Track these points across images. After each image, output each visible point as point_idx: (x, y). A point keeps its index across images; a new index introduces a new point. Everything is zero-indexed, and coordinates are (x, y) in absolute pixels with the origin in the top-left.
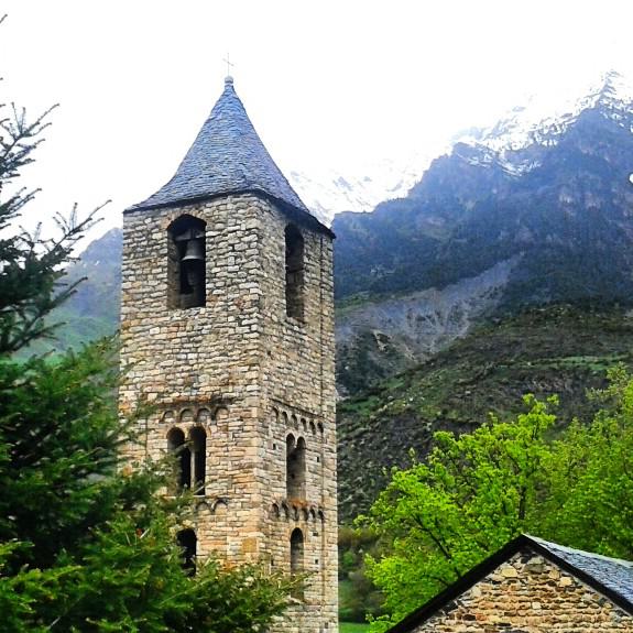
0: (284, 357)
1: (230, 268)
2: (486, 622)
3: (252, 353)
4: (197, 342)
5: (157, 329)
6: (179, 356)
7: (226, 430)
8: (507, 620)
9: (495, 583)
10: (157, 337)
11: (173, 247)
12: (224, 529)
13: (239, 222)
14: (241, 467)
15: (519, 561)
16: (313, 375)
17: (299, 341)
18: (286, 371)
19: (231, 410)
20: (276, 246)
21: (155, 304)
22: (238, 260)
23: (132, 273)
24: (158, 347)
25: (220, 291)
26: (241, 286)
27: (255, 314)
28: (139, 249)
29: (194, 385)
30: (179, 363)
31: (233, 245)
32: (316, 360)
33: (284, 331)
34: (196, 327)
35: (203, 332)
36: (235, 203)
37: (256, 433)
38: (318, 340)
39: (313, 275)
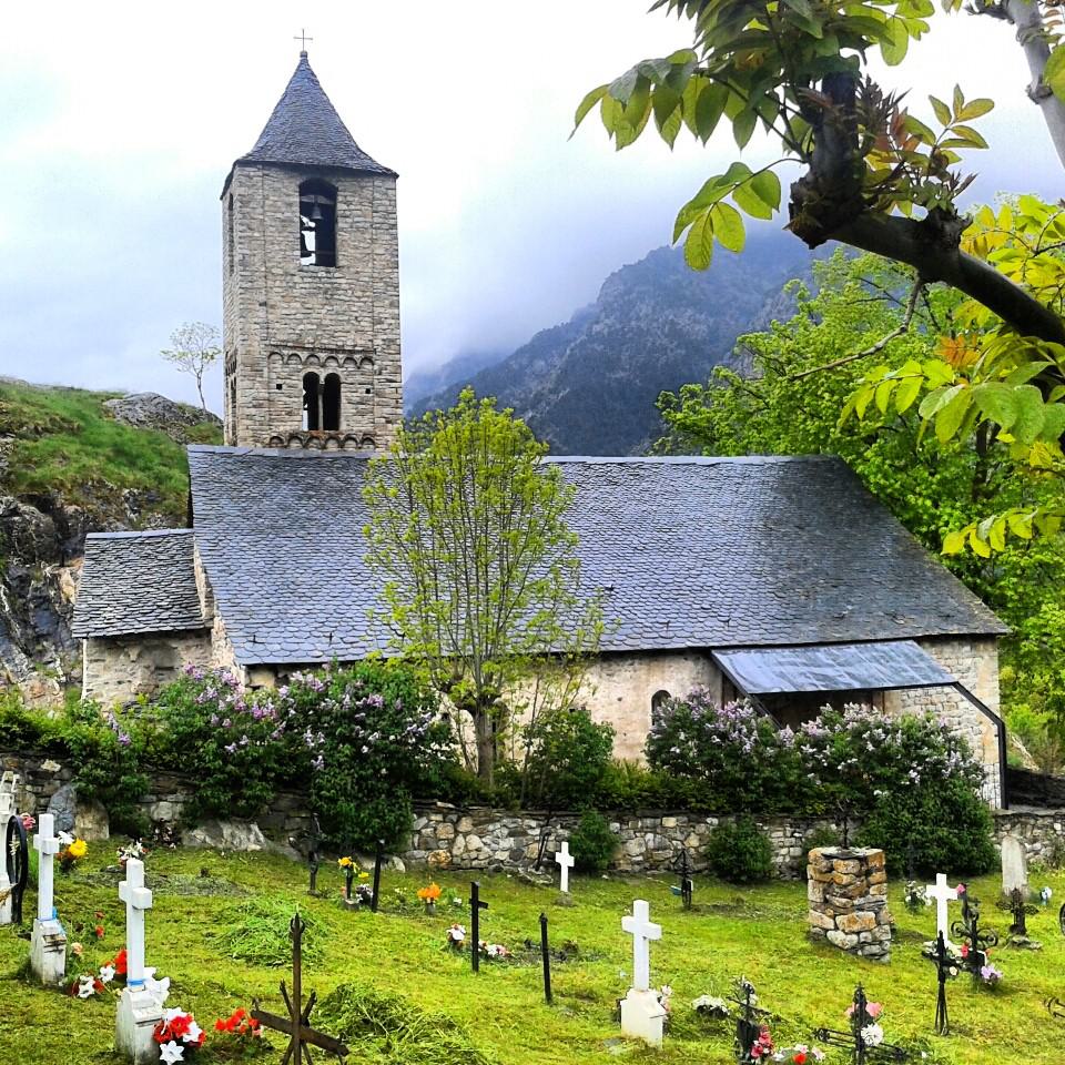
0: (298, 305)
16: (357, 314)
17: (329, 286)
18: (298, 316)
20: (279, 204)
38: (367, 279)
39: (356, 219)
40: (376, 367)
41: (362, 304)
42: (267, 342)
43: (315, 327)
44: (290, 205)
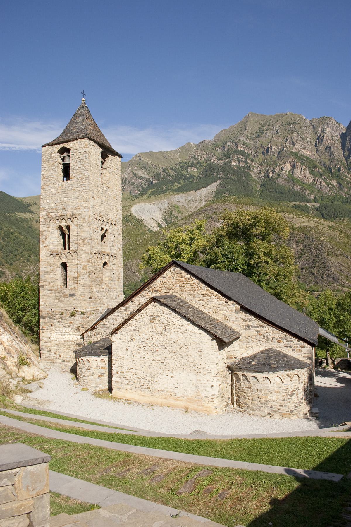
0: (99, 199)
1: (79, 166)
2: (162, 292)
3: (86, 197)
4: (67, 194)
5: (53, 189)
6: (61, 199)
7: (77, 226)
8: (168, 291)
9: (164, 278)
10: (53, 192)
11: (60, 159)
12: (77, 262)
13: (82, 149)
14: (82, 239)
15: (172, 269)
19: (78, 218)
21: (53, 180)
22: (82, 163)
23: (45, 169)
24: (54, 196)
25: (75, 175)
26: (82, 172)
27: (87, 183)
28: (47, 160)
29: (66, 210)
30: (61, 201)
31: (80, 158)
32: (114, 201)
33: (100, 189)
34: (67, 188)
35: (69, 190)
36: (81, 142)
37: (87, 227)
39: (113, 170)
40: (117, 228)
41: (113, 203)
42: (93, 213)
43: (103, 210)
44: (99, 159)
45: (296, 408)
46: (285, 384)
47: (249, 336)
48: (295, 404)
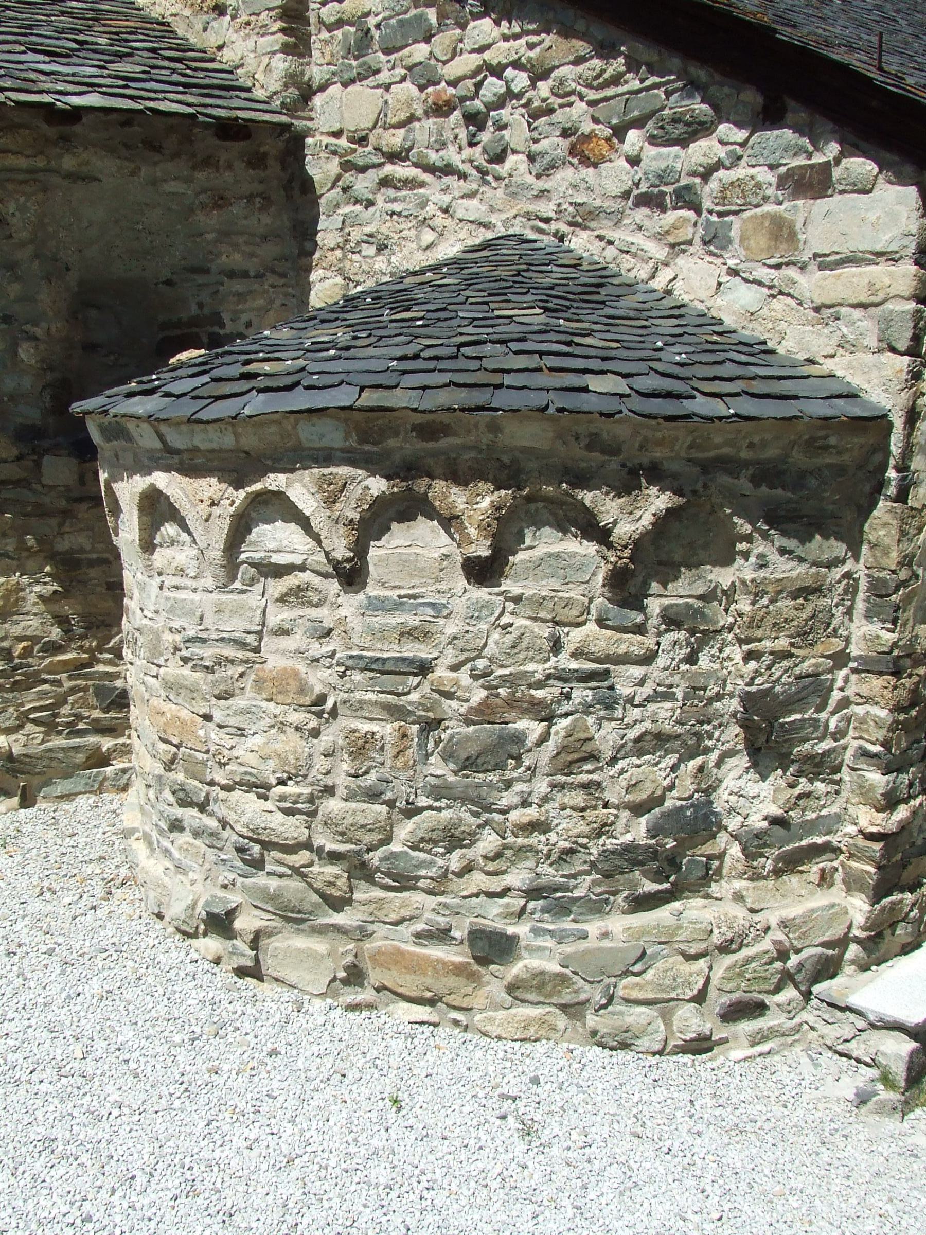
45: (567, 924)
46: (378, 605)
47: (362, 141)
48: (550, 873)
